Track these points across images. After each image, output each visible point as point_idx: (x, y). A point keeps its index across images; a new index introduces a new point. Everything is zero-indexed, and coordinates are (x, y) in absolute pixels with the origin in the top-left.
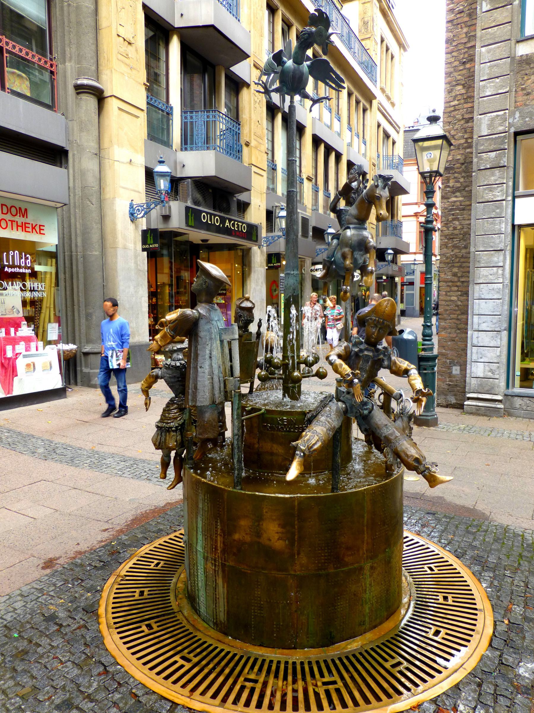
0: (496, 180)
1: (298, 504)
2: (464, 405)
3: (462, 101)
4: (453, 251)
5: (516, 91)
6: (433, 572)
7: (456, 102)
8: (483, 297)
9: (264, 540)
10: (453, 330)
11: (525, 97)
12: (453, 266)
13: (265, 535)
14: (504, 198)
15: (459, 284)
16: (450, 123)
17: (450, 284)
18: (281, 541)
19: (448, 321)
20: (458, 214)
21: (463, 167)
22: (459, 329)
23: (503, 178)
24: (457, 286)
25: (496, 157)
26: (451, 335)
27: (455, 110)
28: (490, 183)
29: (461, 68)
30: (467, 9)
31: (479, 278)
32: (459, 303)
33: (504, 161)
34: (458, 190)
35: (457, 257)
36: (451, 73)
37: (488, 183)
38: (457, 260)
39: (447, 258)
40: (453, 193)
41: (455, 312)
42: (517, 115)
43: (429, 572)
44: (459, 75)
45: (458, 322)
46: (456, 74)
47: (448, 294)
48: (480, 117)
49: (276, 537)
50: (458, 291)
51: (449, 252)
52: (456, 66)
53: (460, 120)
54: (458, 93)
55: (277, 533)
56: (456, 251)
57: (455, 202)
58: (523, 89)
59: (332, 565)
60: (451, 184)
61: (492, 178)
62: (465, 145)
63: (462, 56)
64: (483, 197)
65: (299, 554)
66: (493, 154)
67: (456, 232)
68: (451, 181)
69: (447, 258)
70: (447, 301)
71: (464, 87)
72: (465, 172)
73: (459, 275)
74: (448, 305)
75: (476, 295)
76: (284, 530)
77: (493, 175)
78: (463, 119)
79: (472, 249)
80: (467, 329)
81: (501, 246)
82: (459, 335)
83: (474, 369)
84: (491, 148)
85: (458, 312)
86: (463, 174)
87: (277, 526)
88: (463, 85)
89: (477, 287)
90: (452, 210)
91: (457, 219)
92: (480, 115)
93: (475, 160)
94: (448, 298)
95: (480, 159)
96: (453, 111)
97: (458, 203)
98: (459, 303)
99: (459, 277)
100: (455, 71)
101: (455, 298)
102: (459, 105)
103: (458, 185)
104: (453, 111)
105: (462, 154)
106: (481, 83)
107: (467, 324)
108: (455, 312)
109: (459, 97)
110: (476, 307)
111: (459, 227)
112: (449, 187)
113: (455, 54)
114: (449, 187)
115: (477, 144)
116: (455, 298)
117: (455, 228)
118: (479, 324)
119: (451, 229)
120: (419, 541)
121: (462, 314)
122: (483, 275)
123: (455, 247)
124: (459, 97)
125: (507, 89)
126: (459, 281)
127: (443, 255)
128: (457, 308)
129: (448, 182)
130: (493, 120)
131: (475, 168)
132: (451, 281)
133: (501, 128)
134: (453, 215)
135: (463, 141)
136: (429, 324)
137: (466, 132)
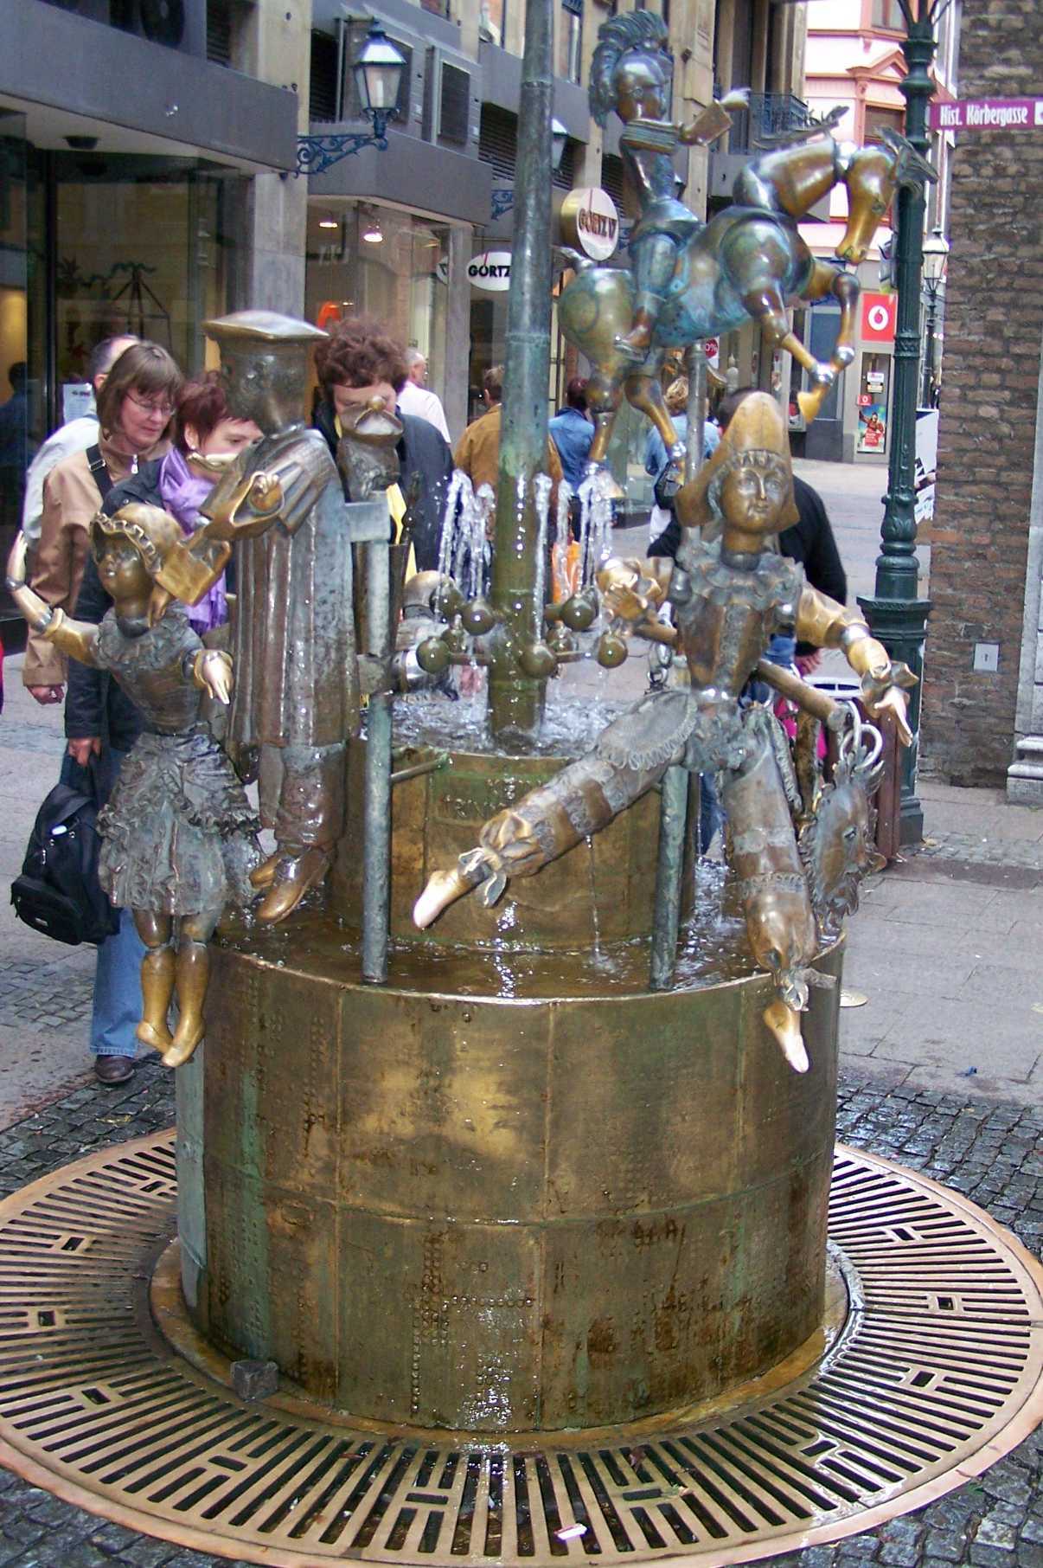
1: (559, 1024)
2: (1006, 775)
6: (910, 1243)
9: (454, 1130)
10: (982, 521)
12: (991, 302)
13: (459, 1117)
15: (1005, 363)
17: (978, 361)
18: (503, 1131)
19: (967, 489)
22: (1001, 518)
24: (999, 370)
26: (975, 538)
32: (1005, 429)
35: (1002, 270)
38: (1004, 282)
39: (971, 272)
40: (1000, 46)
41: (989, 460)
43: (898, 1241)
45: (998, 494)
47: (970, 394)
49: (492, 1117)
50: (1002, 387)
51: (979, 253)
55: (495, 1107)
57: (1003, 79)
59: (644, 1197)
60: (993, 17)
65: (554, 1166)
67: (1004, 184)
69: (971, 272)
70: (965, 420)
73: (1008, 332)
74: (967, 435)
76: (514, 1101)
82: (1001, 539)
85: (1002, 460)
87: (493, 1088)
94: (969, 410)
98: (1005, 429)
99: (1007, 341)
101: (989, 411)
103: (1016, 22)
108: (989, 460)
111: (1013, 169)
112: (984, 24)
116: (992, 412)
117: (1000, 172)
120: (866, 1165)
121: (1014, 466)
123: (998, 235)
126: (1006, 353)
127: (959, 259)
128: (996, 446)
136: (904, 498)
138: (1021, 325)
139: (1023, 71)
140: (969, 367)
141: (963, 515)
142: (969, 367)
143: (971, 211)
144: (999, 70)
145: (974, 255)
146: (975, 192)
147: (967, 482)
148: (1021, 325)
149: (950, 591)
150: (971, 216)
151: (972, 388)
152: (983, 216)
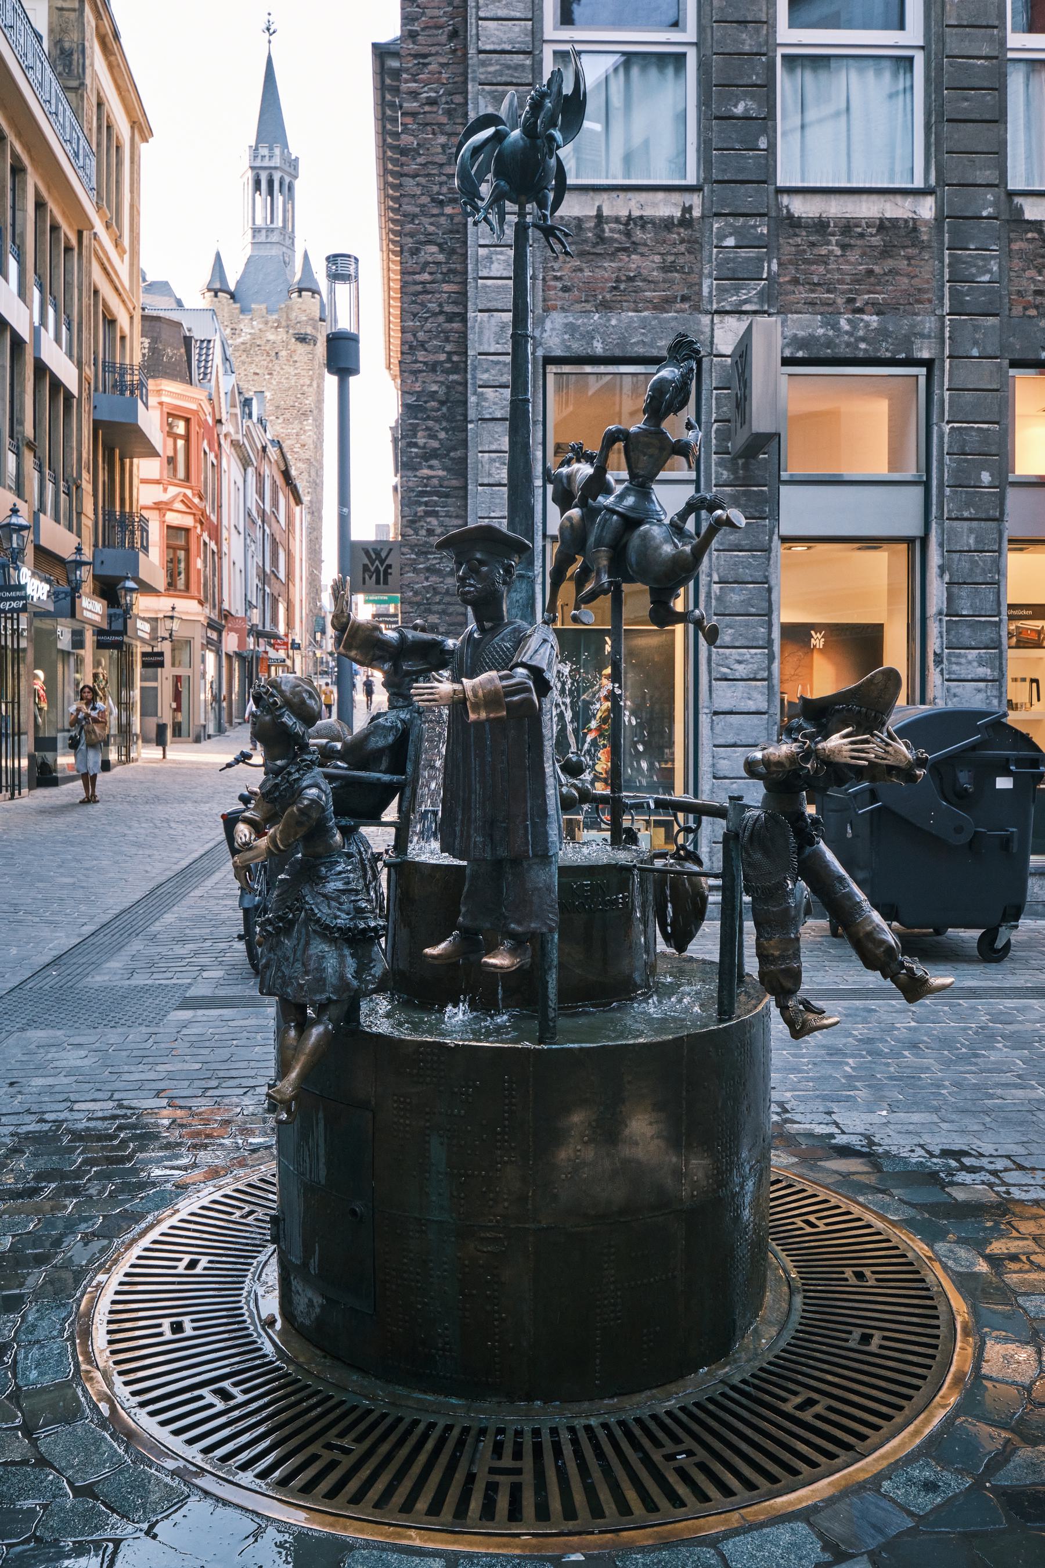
4: (427, 579)
5: (544, 279)
7: (426, 277)
12: (430, 611)
16: (415, 315)
20: (436, 504)
21: (444, 409)
27: (426, 292)
30: (444, 100)
34: (433, 454)
35: (436, 591)
36: (415, 216)
37: (498, 448)
38: (437, 599)
44: (431, 224)
46: (425, 220)
52: (424, 206)
53: (435, 315)
54: (430, 259)
56: (434, 579)
57: (429, 478)
62: (448, 365)
63: (436, 188)
64: (490, 475)
68: (420, 434)
69: (416, 593)
71: (442, 250)
72: (447, 421)
78: (441, 312)
86: (444, 424)
88: (439, 245)
90: (423, 494)
91: (435, 514)
93: (472, 399)
96: (420, 293)
97: (435, 481)
100: (423, 213)
102: (432, 282)
103: (435, 444)
104: (420, 293)
105: (442, 383)
106: (482, 252)
109: (432, 268)
111: (439, 531)
112: (415, 445)
113: (422, 180)
114: (415, 445)
115: (475, 369)
117: (430, 532)
119: (423, 532)
124: (432, 268)
129: (415, 436)
131: (472, 414)
134: (426, 504)
135: (443, 357)
137: (447, 340)
138: (450, 625)
139: (441, 473)
144: (426, 472)
148: (450, 625)
152: (422, 560)
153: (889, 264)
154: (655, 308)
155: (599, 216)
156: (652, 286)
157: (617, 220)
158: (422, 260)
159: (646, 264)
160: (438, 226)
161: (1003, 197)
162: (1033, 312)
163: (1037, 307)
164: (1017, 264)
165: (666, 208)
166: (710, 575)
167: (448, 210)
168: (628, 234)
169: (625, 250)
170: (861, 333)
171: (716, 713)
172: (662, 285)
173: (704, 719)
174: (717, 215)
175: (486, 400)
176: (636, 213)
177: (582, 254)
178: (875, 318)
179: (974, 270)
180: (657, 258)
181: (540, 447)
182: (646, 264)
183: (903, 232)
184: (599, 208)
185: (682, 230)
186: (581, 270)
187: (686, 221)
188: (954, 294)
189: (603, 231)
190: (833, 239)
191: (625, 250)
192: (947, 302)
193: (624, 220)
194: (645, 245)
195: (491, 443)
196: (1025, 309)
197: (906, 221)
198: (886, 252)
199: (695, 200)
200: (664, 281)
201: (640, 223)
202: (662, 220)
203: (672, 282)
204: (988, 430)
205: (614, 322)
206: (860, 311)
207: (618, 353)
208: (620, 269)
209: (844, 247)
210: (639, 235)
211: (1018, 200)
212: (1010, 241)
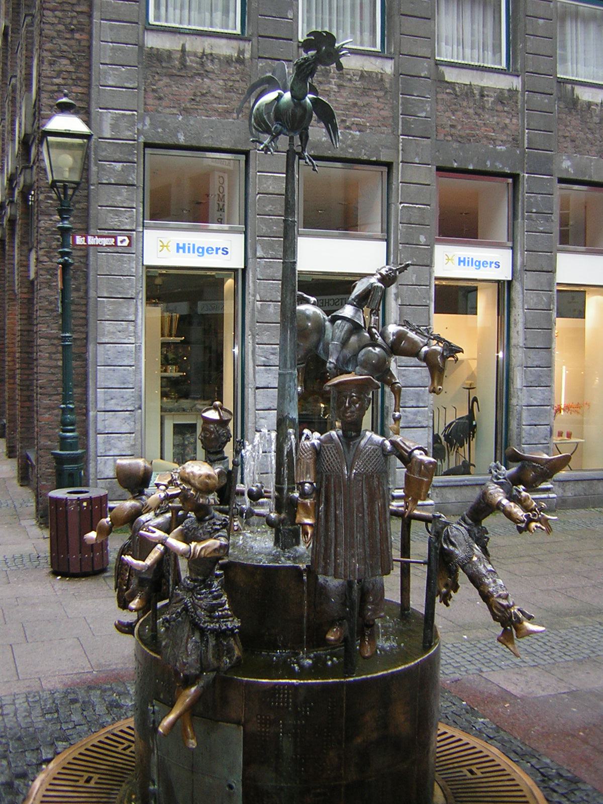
0: (124, 202)
3: (70, 82)
5: (145, 90)
8: (109, 362)
11: (157, 102)
14: (134, 227)
23: (132, 201)
25: (123, 170)
28: (116, 204)
29: (68, 36)
31: (103, 335)
33: (132, 179)
36: (54, 38)
42: (148, 121)
44: (65, 44)
46: (60, 42)
47: (54, 356)
48: (100, 110)
52: (60, 31)
58: (153, 90)
61: (118, 198)
63: (68, 21)
64: (106, 222)
66: (119, 166)
70: (51, 367)
74: (53, 374)
75: (100, 360)
77: (120, 194)
79: (92, 293)
80: (87, 409)
81: (131, 293)
83: (100, 467)
84: (117, 156)
88: (70, 59)
89: (100, 348)
92: (101, 108)
95: (101, 169)
107: (86, 401)
109: (65, 75)
110: (100, 376)
113: (58, 13)
118: (106, 401)
122: (109, 332)
124: (65, 75)
125: (136, 85)
130: (117, 119)
132: (57, 338)
133: (128, 134)
140: (52, 344)
141: (53, 409)
142: (52, 344)
143: (49, 277)
145: (52, 296)
146: (51, 269)
147: (54, 395)
149: (49, 443)
150: (50, 279)
151: (54, 353)
153: (366, 100)
154: (220, 115)
155: (183, 50)
156: (218, 101)
157: (195, 55)
158: (57, 69)
159: (214, 85)
160: (70, 46)
161: (433, 64)
162: (450, 138)
163: (452, 136)
164: (441, 107)
165: (226, 49)
166: (254, 296)
167: (77, 36)
168: (202, 64)
169: (199, 74)
170: (349, 142)
171: (257, 388)
172: (224, 101)
173: (249, 392)
174: (260, 57)
175: (104, 170)
176: (208, 51)
177: (171, 76)
178: (358, 133)
179: (416, 109)
180: (221, 82)
181: (142, 204)
182: (214, 85)
183: (375, 80)
184: (183, 46)
185: (238, 65)
186: (170, 86)
187: (240, 61)
188: (405, 122)
189: (186, 61)
190: (333, 81)
191: (199, 74)
192: (400, 127)
193: (200, 55)
194: (213, 72)
195: (107, 200)
196: (445, 135)
197: (377, 74)
198: (365, 92)
199: (247, 46)
200: (226, 98)
201: (210, 58)
202: (225, 57)
203: (231, 99)
204: (424, 209)
205: (192, 122)
206: (349, 128)
207: (194, 143)
208: (196, 87)
209: (340, 86)
210: (210, 66)
211: (442, 68)
212: (437, 93)
